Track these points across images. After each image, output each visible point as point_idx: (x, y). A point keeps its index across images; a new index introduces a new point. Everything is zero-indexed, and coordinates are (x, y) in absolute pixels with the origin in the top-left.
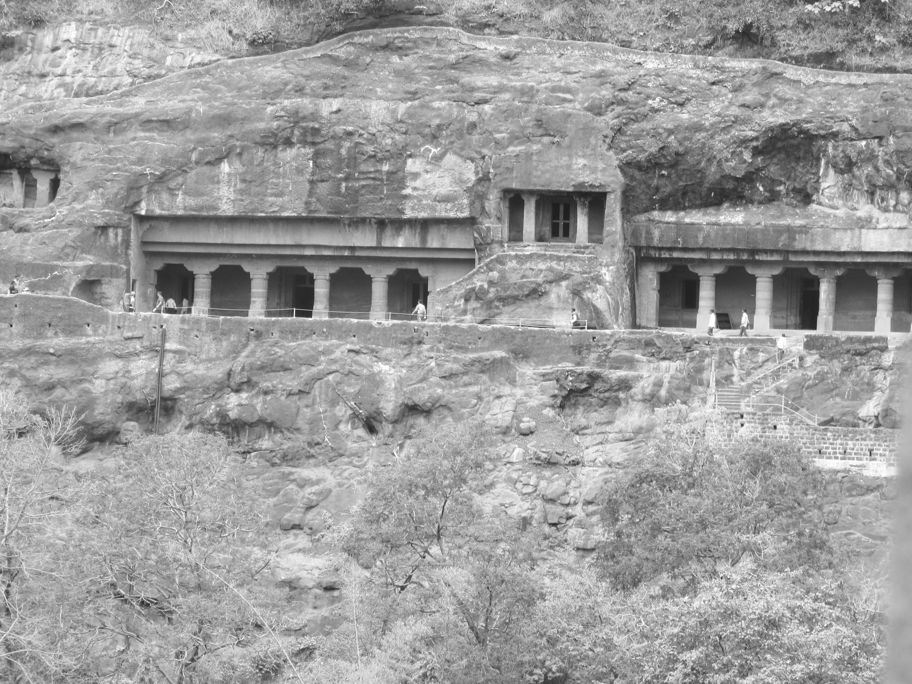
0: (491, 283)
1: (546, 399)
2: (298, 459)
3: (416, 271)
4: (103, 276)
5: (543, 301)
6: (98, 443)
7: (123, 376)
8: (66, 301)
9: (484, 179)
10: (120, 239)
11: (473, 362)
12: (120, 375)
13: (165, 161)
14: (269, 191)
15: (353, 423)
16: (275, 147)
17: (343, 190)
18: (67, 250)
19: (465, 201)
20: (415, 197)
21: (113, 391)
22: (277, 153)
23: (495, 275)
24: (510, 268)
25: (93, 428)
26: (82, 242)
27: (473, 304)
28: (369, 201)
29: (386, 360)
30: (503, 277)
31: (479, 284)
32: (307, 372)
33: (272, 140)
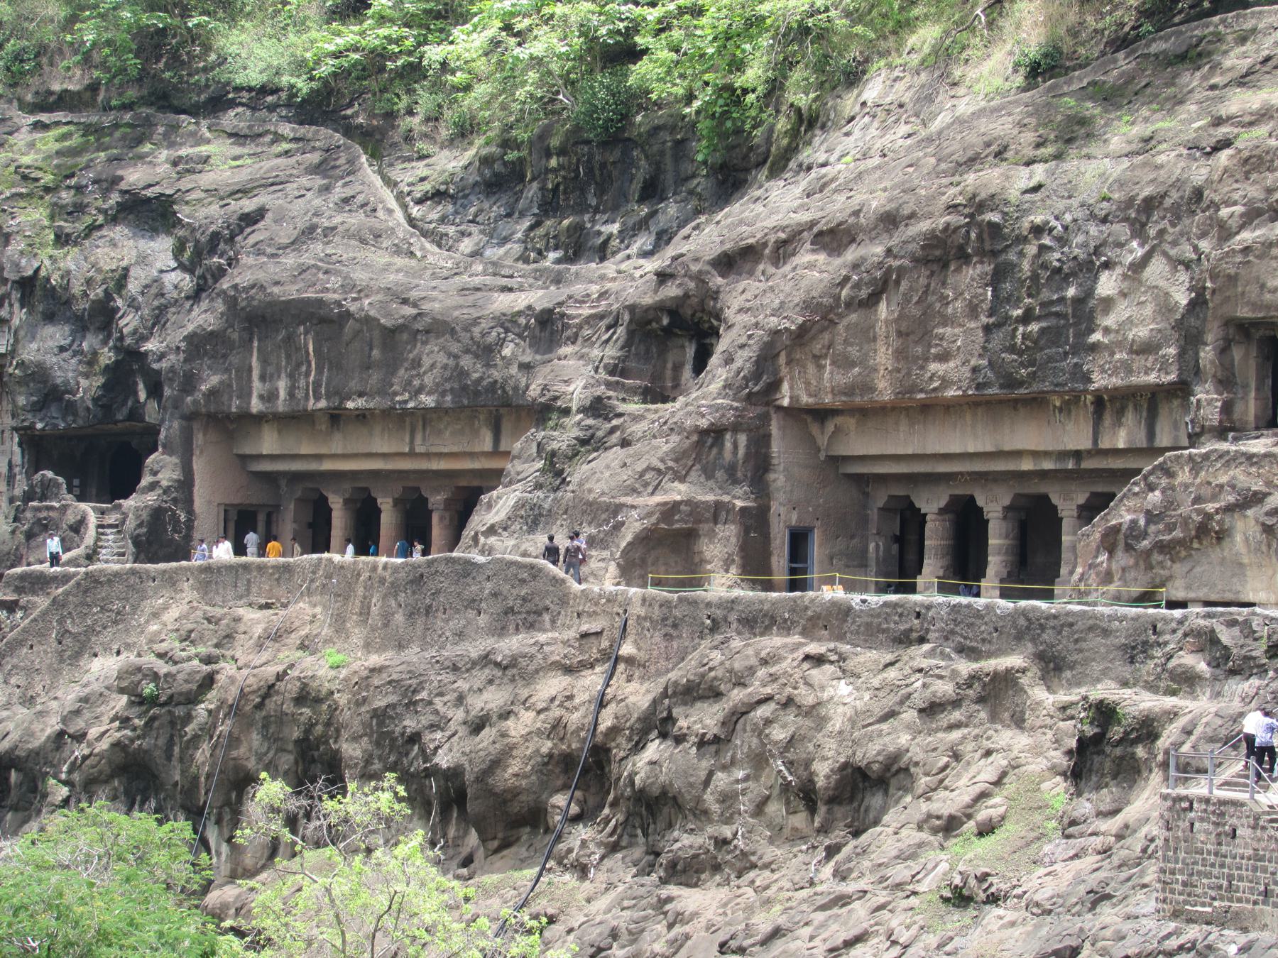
0: (1151, 517)
1: (1059, 758)
2: (697, 872)
3: (972, 499)
4: (700, 522)
5: (1226, 551)
6: (528, 829)
7: (561, 705)
8: (532, 567)
9: (1199, 303)
10: (741, 451)
11: (973, 678)
12: (557, 703)
13: (807, 305)
14: (933, 351)
15: (788, 803)
16: (945, 266)
17: (1019, 340)
18: (647, 476)
19: (1172, 351)
20: (1106, 347)
21: (539, 732)
22: (946, 276)
23: (1155, 497)
24: (1180, 484)
25: (505, 802)
26: (676, 460)
27: (1123, 559)
28: (1051, 359)
29: (853, 675)
30: (1170, 504)
31: (1128, 517)
32: (737, 696)
33: (938, 253)
